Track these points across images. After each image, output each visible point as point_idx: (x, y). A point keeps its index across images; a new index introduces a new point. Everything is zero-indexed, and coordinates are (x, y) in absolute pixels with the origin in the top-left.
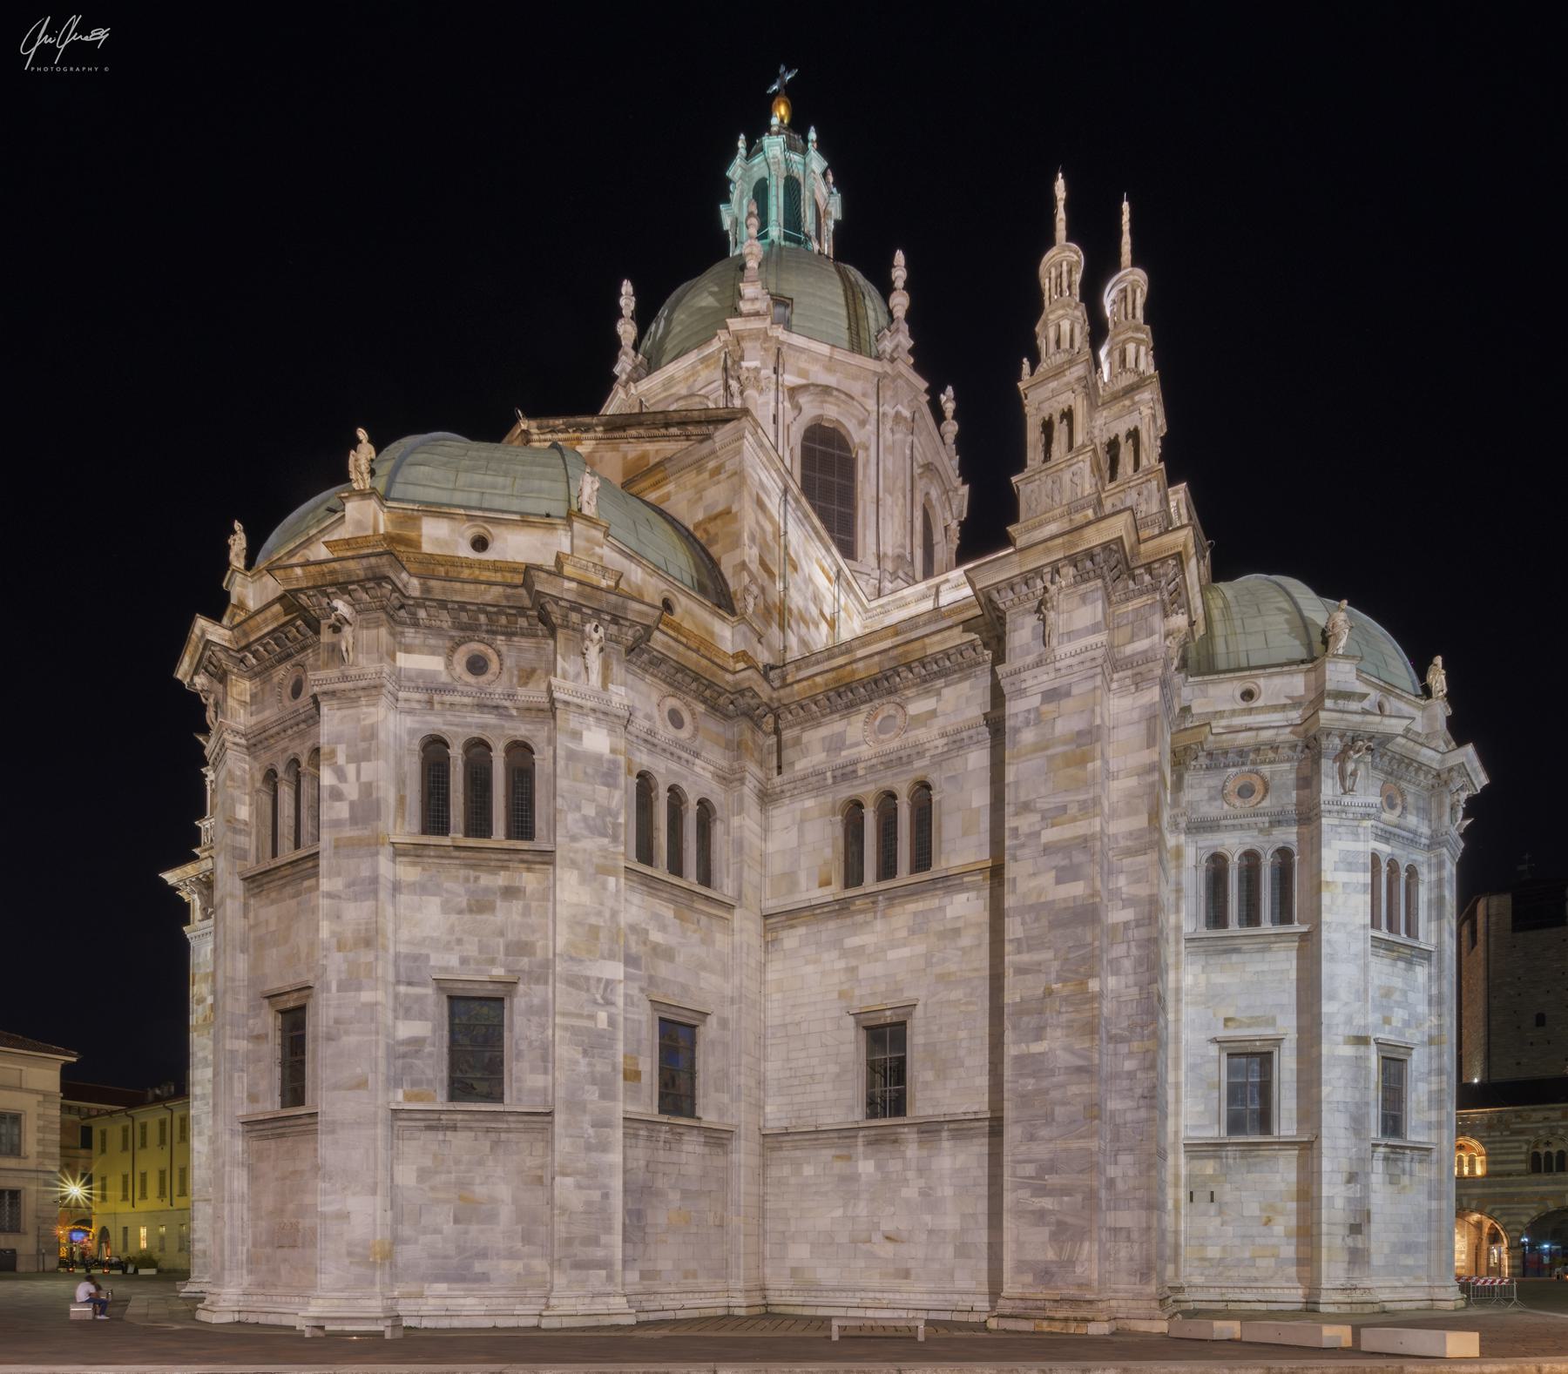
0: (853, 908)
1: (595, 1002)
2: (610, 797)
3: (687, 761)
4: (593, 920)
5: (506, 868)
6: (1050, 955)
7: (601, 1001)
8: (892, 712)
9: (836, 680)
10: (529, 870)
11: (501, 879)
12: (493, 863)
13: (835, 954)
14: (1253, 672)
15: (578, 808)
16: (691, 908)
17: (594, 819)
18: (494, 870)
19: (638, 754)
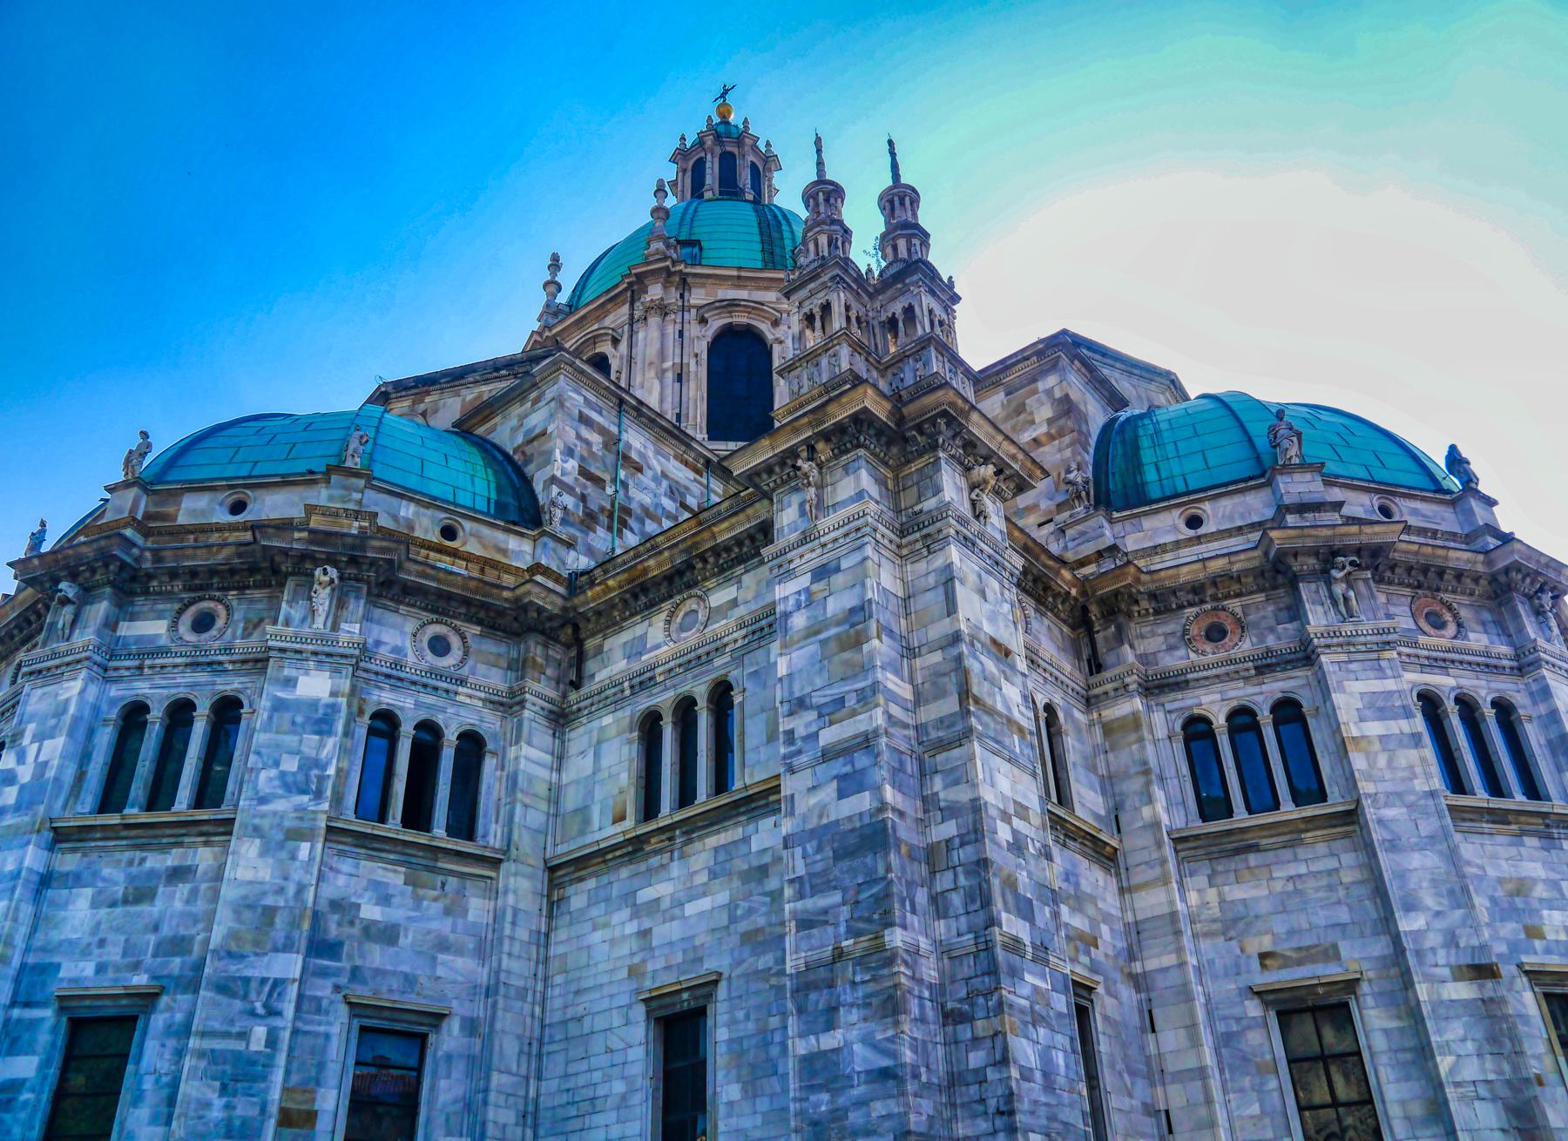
0: (648, 848)
1: (253, 1013)
2: (321, 745)
3: (447, 691)
4: (269, 901)
5: (180, 845)
6: (836, 897)
7: (260, 1010)
8: (694, 607)
9: (630, 581)
10: (206, 844)
11: (172, 859)
12: (165, 840)
13: (625, 913)
14: (1192, 497)
15: (277, 764)
16: (433, 870)
17: (294, 774)
18: (164, 849)
19: (376, 692)
